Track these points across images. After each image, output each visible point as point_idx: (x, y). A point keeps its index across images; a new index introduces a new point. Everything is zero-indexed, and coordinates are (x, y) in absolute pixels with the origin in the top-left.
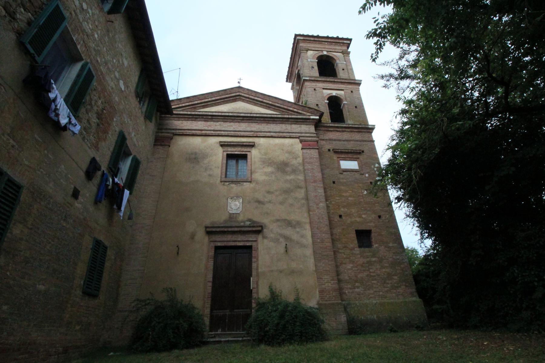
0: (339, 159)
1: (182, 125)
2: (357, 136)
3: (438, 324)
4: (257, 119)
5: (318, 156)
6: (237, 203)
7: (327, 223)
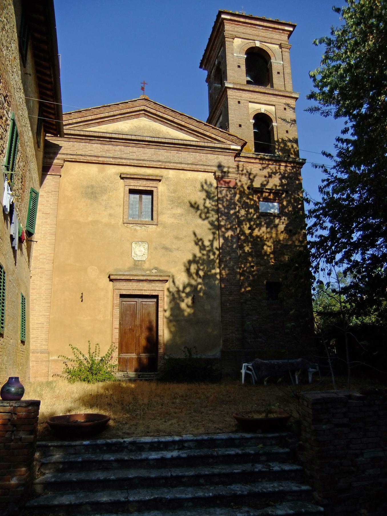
4: (166, 145)
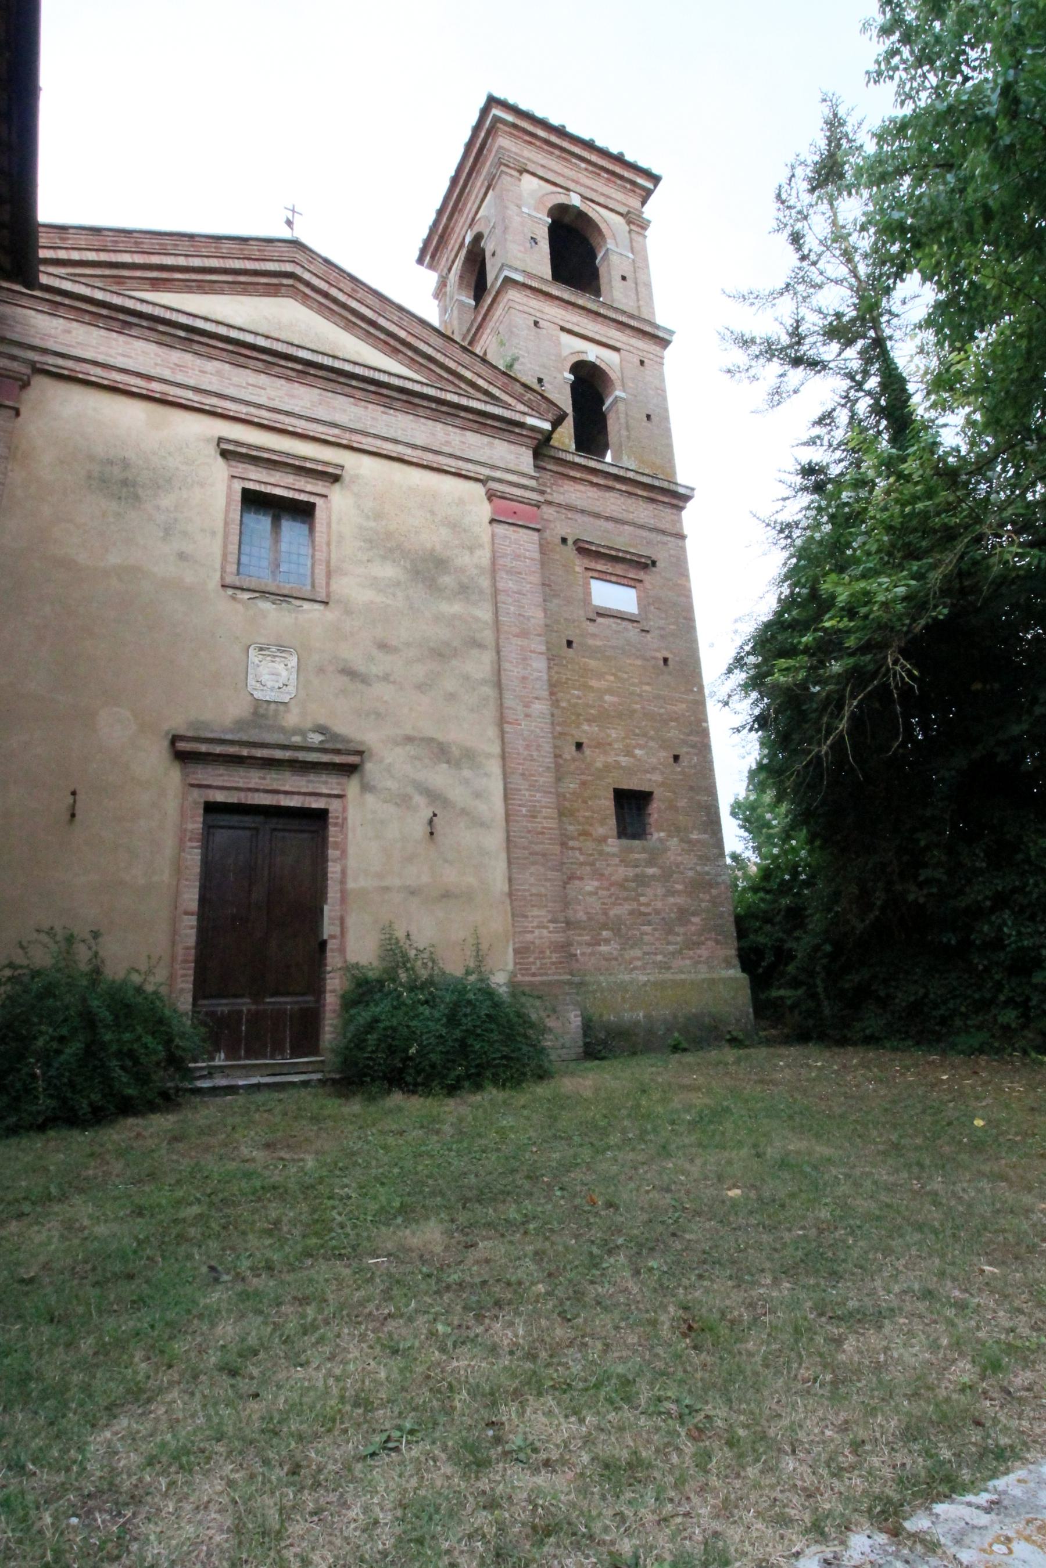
0: (591, 574)
1: (66, 339)
2: (643, 512)
3: (773, 1032)
4: (354, 383)
5: (537, 555)
6: (280, 667)
7: (549, 760)
